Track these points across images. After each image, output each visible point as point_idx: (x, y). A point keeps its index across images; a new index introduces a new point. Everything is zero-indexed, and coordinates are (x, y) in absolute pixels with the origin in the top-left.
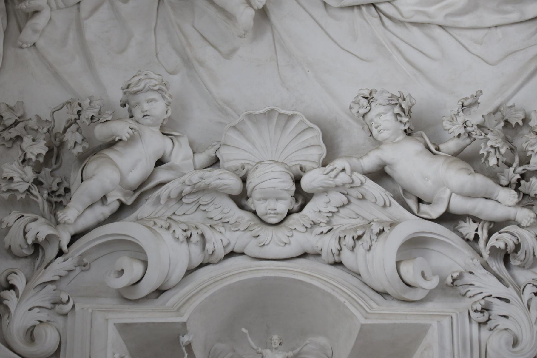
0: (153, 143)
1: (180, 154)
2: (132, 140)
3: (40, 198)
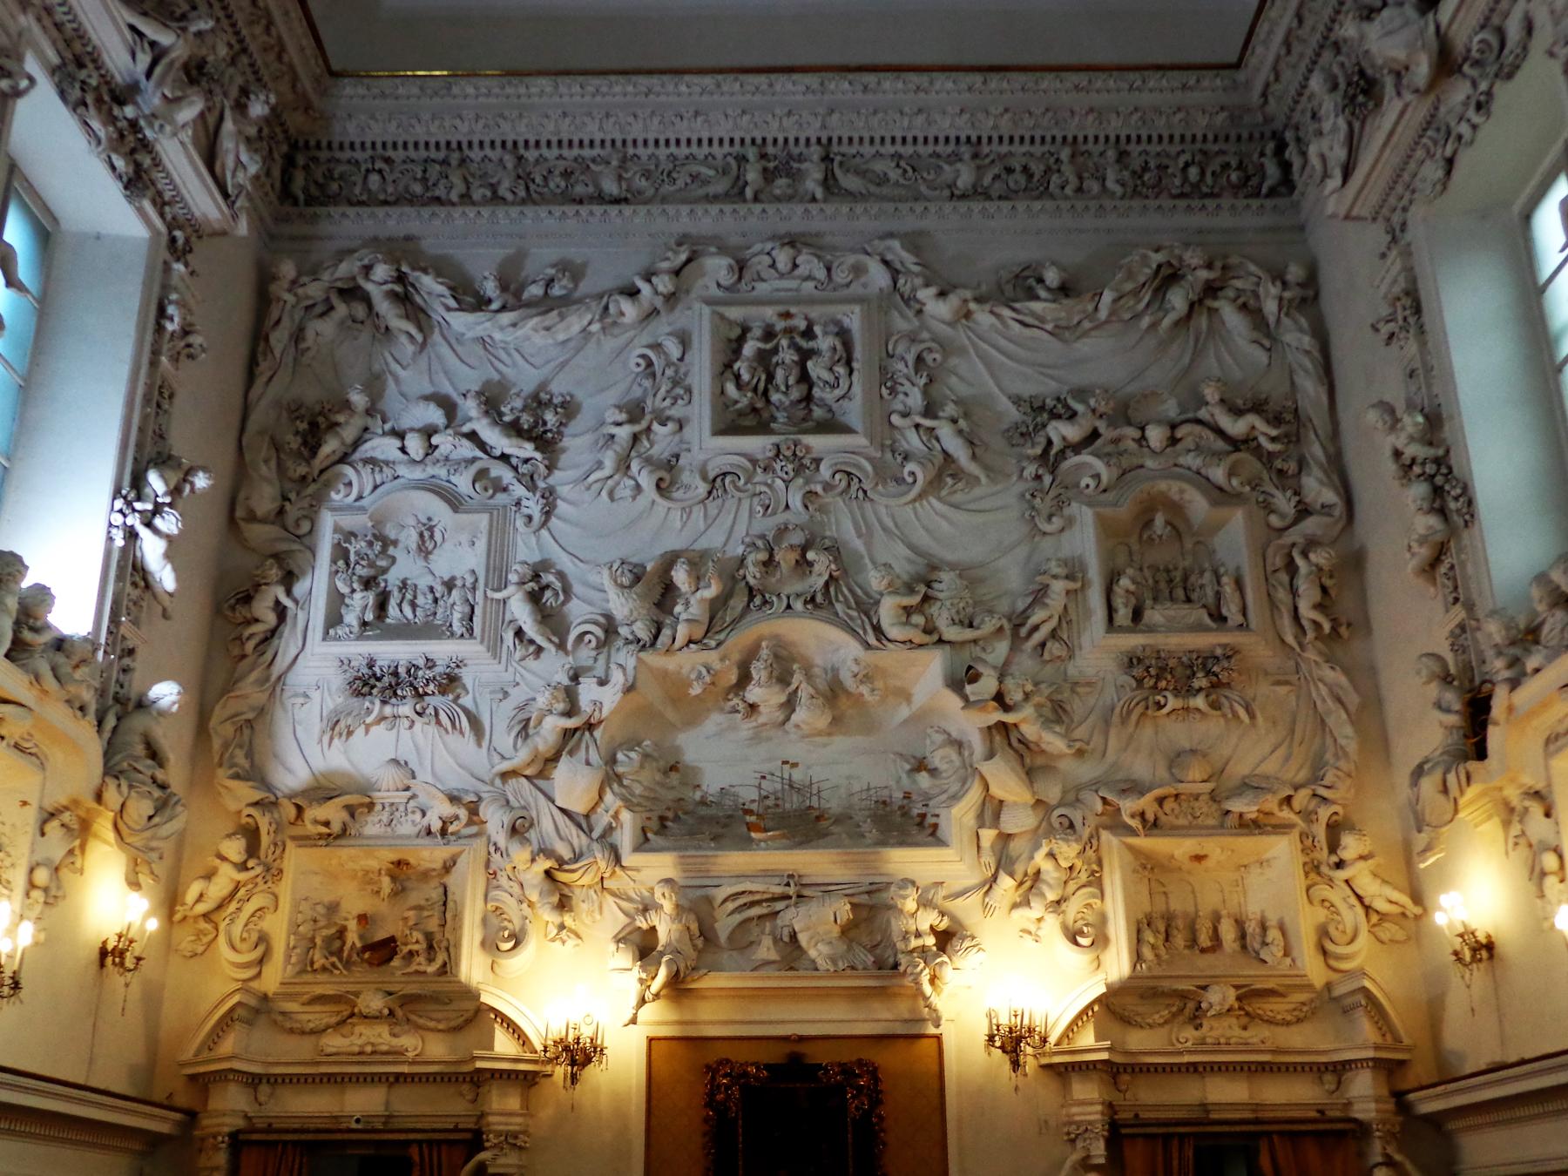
2: (347, 423)
3: (306, 453)
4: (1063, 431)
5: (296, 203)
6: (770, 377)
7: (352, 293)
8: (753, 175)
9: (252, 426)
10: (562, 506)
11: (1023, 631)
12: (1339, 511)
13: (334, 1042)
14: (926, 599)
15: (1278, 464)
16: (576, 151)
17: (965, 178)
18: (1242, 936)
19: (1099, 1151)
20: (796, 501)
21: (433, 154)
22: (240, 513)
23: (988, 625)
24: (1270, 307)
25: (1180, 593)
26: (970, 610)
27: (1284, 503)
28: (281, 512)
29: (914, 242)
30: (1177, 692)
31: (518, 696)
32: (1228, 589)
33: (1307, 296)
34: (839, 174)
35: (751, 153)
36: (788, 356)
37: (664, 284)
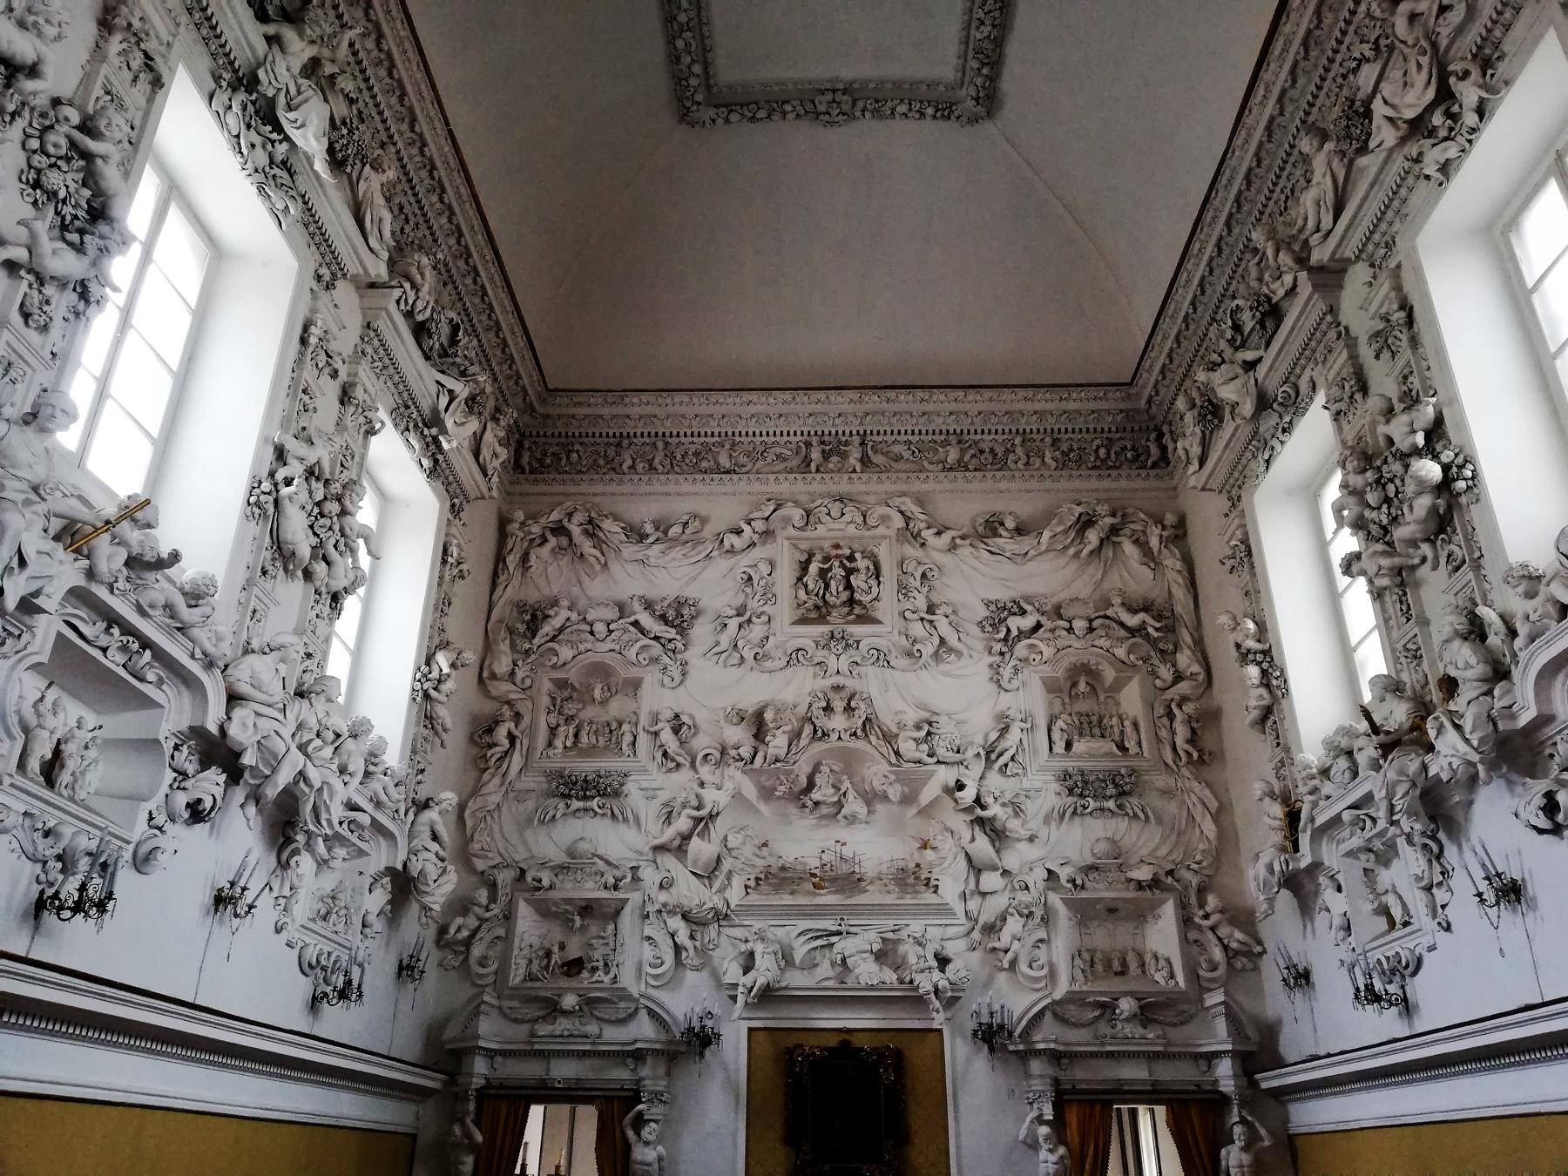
0: (564, 614)
1: (574, 617)
4: (1015, 623)
5: (523, 472)
6: (827, 587)
7: (559, 530)
8: (816, 455)
9: (494, 617)
10: (693, 673)
11: (993, 757)
12: (1201, 678)
13: (543, 1029)
14: (929, 733)
15: (1161, 645)
16: (702, 439)
17: (953, 455)
18: (1143, 965)
19: (1049, 1115)
20: (844, 667)
21: (611, 440)
22: (485, 674)
23: (970, 753)
24: (1154, 542)
25: (1097, 731)
26: (958, 742)
27: (1166, 673)
28: (513, 673)
29: (920, 502)
30: (1095, 797)
31: (663, 796)
32: (1129, 730)
33: (1179, 534)
34: (870, 454)
35: (814, 440)
36: (838, 572)
37: (759, 526)
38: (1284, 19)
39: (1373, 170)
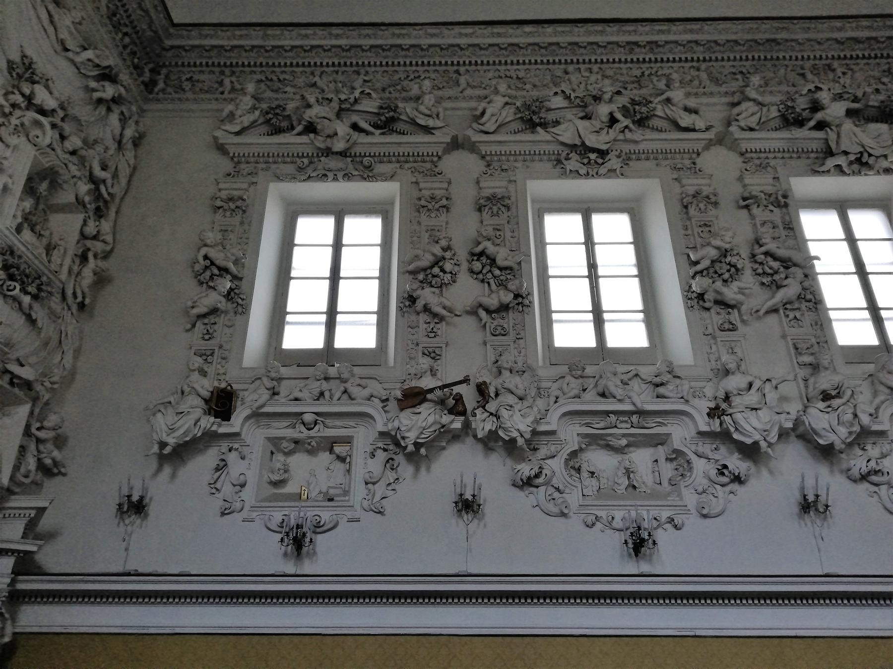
38: (515, 26)
39: (543, 139)
